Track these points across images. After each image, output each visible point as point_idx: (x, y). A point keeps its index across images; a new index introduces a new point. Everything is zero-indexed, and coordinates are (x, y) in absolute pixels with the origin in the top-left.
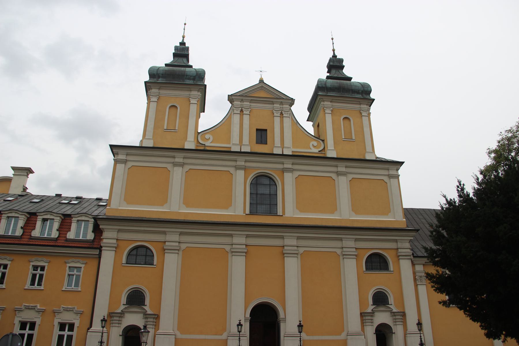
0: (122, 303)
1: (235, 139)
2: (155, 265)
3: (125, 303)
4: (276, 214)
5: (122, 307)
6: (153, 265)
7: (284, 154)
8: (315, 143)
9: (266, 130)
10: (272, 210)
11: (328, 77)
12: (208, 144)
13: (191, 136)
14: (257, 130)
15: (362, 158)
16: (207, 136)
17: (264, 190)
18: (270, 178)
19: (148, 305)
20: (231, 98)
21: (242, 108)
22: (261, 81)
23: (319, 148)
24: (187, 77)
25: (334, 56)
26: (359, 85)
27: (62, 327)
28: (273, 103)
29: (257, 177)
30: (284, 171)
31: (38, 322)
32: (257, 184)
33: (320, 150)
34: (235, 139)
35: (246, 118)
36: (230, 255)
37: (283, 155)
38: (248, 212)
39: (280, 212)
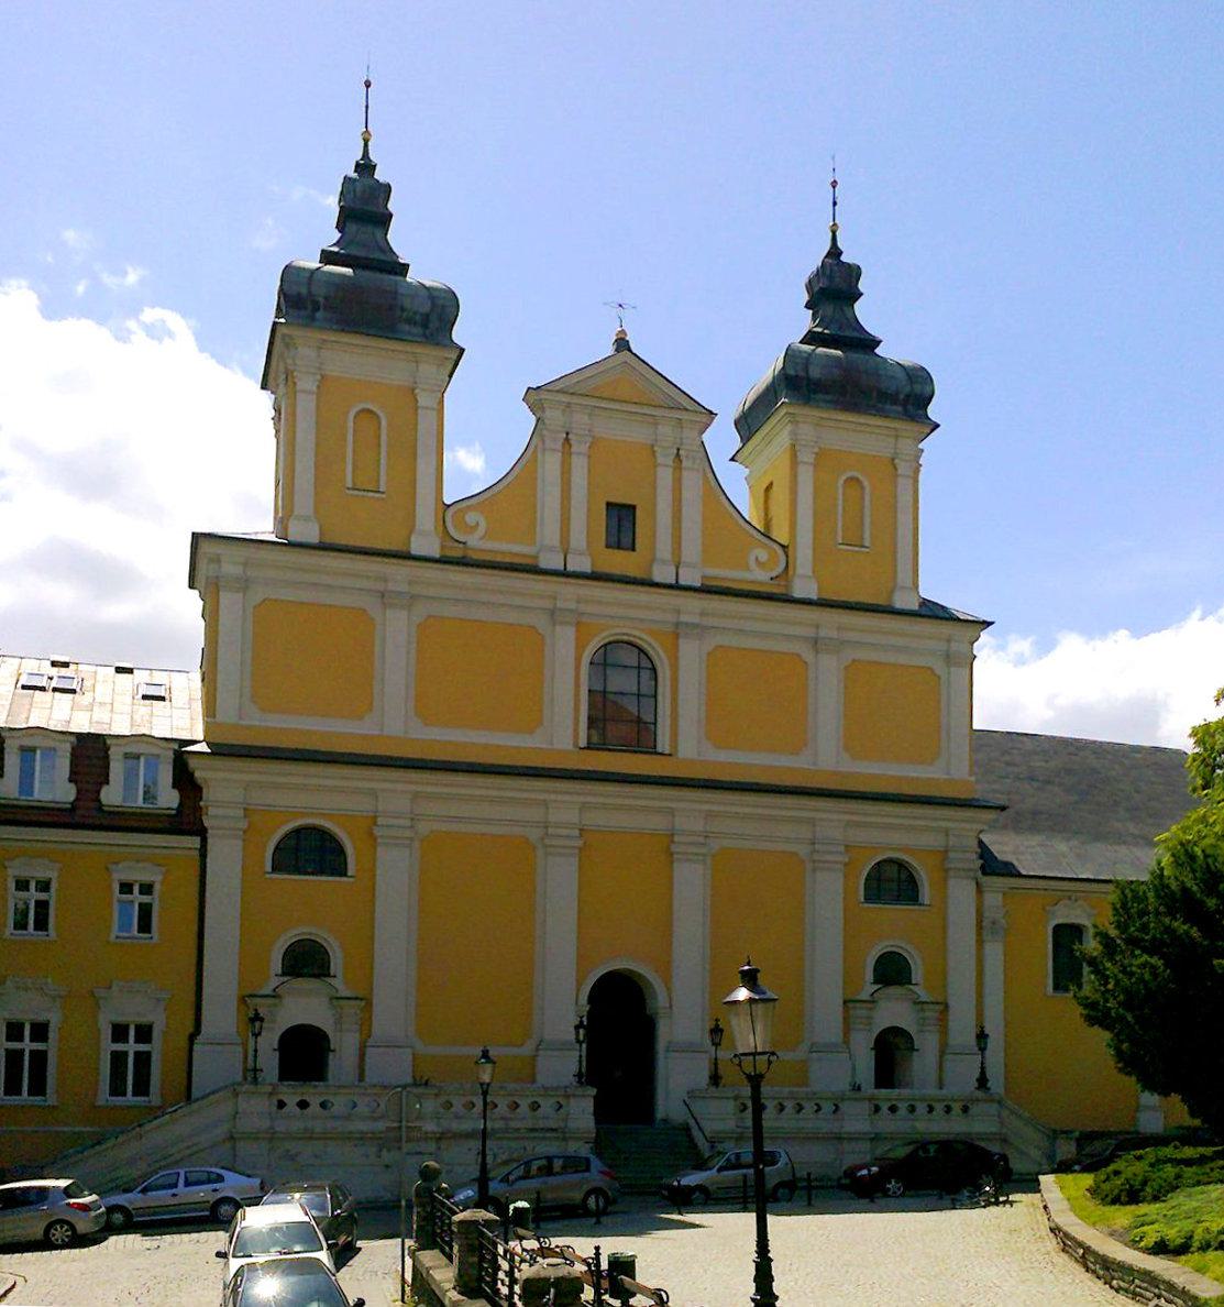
0: (272, 973)
1: (550, 532)
2: (351, 877)
3: (280, 972)
4: (653, 751)
5: (275, 982)
6: (345, 875)
7: (682, 582)
8: (763, 555)
9: (634, 507)
10: (641, 738)
11: (810, 338)
12: (473, 541)
13: (425, 518)
14: (609, 505)
15: (881, 601)
16: (471, 518)
17: (620, 682)
18: (641, 650)
19: (340, 975)
20: (536, 398)
21: (567, 434)
22: (622, 344)
23: (772, 570)
24: (405, 314)
25: (835, 252)
26: (901, 375)
27: (119, 1032)
28: (655, 422)
29: (605, 645)
30: (677, 631)
31: (54, 1019)
32: (605, 664)
33: (774, 574)
34: (550, 532)
35: (579, 466)
36: (540, 853)
37: (676, 587)
38: (583, 742)
39: (663, 744)
